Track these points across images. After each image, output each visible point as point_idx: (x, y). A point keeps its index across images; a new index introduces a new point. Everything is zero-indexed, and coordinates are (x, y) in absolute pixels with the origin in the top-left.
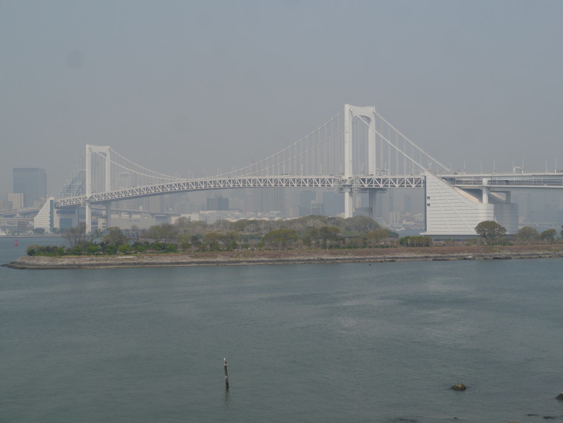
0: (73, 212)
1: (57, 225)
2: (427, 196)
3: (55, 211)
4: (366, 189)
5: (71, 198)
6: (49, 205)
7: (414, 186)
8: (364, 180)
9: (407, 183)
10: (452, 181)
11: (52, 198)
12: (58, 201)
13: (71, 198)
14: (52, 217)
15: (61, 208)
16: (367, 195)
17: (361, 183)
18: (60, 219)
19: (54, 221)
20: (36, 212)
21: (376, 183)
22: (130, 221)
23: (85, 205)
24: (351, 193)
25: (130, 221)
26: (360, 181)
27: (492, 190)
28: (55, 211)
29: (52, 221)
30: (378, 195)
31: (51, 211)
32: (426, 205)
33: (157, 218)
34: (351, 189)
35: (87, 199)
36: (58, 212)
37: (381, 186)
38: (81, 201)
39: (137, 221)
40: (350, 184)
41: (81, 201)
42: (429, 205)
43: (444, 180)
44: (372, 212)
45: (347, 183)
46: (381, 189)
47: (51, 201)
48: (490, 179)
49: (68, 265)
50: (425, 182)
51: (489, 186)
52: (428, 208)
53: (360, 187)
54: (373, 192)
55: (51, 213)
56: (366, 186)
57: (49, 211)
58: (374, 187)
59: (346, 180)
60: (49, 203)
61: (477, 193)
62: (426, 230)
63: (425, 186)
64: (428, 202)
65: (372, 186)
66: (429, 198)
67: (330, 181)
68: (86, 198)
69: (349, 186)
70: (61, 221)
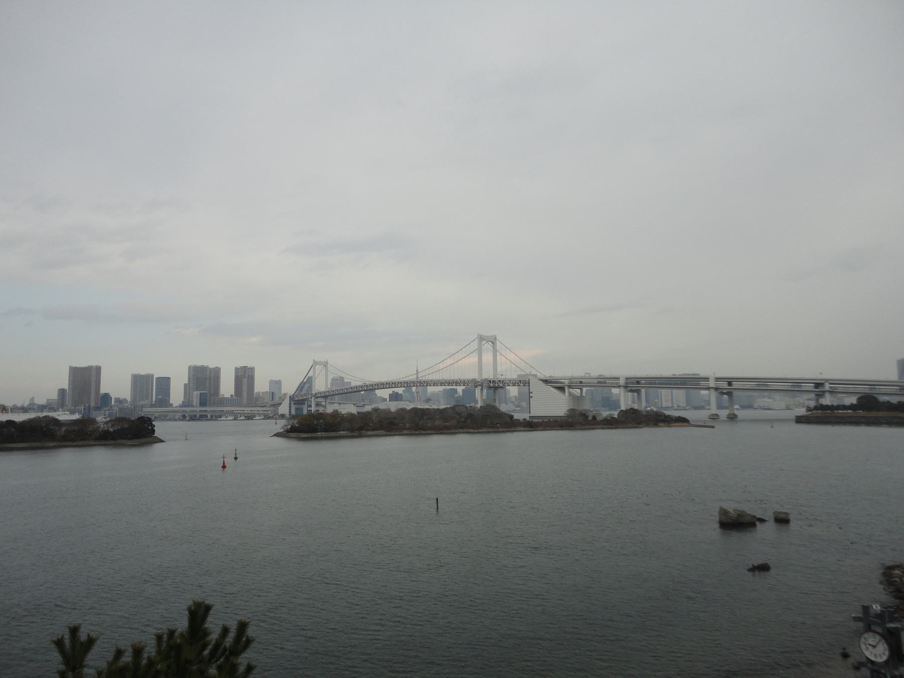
0: (304, 404)
1: (293, 412)
2: (531, 391)
3: (292, 403)
4: (492, 387)
7: (522, 385)
8: (490, 381)
9: (518, 383)
14: (290, 407)
15: (297, 401)
16: (492, 391)
20: (280, 404)
21: (498, 383)
23: (311, 398)
28: (292, 403)
29: (290, 410)
30: (500, 390)
32: (530, 397)
33: (357, 406)
34: (482, 387)
35: (313, 395)
36: (294, 404)
37: (501, 385)
41: (309, 397)
42: (532, 397)
46: (501, 387)
47: (290, 397)
49: (307, 437)
50: (529, 383)
54: (496, 388)
55: (290, 404)
56: (492, 385)
57: (289, 403)
59: (479, 382)
61: (561, 389)
62: (530, 413)
63: (529, 385)
66: (532, 392)
68: (312, 394)
70: (296, 409)
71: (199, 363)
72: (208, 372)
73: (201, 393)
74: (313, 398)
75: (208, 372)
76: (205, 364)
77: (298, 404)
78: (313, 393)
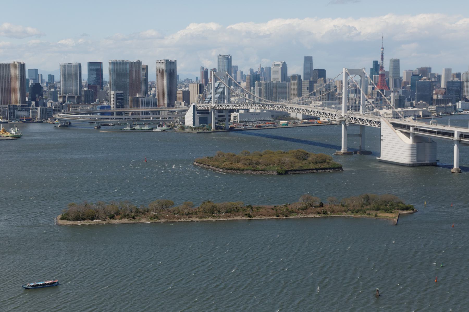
2: (382, 134)
3: (196, 112)
5: (205, 105)
6: (193, 108)
8: (352, 118)
10: (395, 125)
11: (193, 104)
12: (198, 106)
13: (205, 105)
14: (194, 116)
17: (351, 120)
18: (200, 118)
19: (196, 119)
22: (253, 114)
24: (345, 125)
25: (253, 114)
26: (350, 119)
27: (416, 134)
28: (196, 112)
29: (194, 119)
31: (193, 112)
37: (361, 123)
38: (209, 108)
39: (258, 114)
40: (345, 120)
43: (391, 125)
44: (361, 137)
45: (344, 119)
47: (194, 106)
48: (416, 127)
51: (413, 132)
52: (382, 142)
53: (350, 122)
55: (194, 114)
56: (353, 122)
57: (193, 112)
58: (357, 123)
59: (343, 117)
60: (193, 107)
61: (408, 135)
64: (382, 138)
65: (356, 122)
67: (336, 115)
69: (345, 121)
71: (119, 58)
72: (128, 67)
73: (117, 94)
74: (212, 110)
75: (128, 67)
76: (126, 59)
77: (202, 113)
78: (212, 105)
